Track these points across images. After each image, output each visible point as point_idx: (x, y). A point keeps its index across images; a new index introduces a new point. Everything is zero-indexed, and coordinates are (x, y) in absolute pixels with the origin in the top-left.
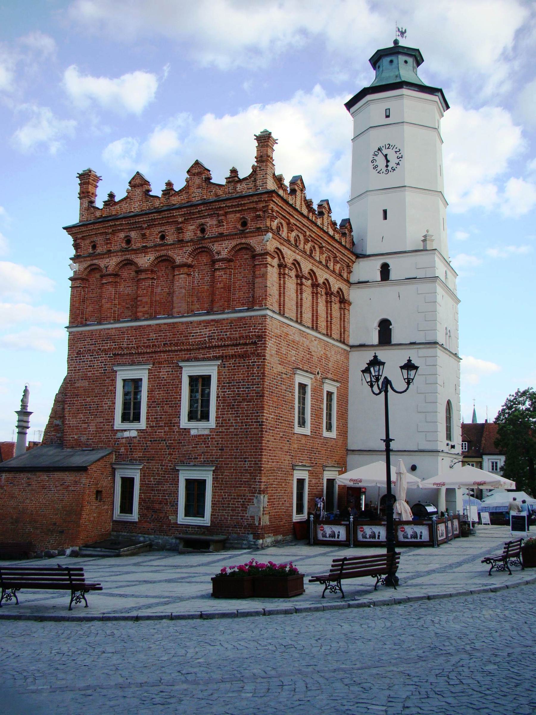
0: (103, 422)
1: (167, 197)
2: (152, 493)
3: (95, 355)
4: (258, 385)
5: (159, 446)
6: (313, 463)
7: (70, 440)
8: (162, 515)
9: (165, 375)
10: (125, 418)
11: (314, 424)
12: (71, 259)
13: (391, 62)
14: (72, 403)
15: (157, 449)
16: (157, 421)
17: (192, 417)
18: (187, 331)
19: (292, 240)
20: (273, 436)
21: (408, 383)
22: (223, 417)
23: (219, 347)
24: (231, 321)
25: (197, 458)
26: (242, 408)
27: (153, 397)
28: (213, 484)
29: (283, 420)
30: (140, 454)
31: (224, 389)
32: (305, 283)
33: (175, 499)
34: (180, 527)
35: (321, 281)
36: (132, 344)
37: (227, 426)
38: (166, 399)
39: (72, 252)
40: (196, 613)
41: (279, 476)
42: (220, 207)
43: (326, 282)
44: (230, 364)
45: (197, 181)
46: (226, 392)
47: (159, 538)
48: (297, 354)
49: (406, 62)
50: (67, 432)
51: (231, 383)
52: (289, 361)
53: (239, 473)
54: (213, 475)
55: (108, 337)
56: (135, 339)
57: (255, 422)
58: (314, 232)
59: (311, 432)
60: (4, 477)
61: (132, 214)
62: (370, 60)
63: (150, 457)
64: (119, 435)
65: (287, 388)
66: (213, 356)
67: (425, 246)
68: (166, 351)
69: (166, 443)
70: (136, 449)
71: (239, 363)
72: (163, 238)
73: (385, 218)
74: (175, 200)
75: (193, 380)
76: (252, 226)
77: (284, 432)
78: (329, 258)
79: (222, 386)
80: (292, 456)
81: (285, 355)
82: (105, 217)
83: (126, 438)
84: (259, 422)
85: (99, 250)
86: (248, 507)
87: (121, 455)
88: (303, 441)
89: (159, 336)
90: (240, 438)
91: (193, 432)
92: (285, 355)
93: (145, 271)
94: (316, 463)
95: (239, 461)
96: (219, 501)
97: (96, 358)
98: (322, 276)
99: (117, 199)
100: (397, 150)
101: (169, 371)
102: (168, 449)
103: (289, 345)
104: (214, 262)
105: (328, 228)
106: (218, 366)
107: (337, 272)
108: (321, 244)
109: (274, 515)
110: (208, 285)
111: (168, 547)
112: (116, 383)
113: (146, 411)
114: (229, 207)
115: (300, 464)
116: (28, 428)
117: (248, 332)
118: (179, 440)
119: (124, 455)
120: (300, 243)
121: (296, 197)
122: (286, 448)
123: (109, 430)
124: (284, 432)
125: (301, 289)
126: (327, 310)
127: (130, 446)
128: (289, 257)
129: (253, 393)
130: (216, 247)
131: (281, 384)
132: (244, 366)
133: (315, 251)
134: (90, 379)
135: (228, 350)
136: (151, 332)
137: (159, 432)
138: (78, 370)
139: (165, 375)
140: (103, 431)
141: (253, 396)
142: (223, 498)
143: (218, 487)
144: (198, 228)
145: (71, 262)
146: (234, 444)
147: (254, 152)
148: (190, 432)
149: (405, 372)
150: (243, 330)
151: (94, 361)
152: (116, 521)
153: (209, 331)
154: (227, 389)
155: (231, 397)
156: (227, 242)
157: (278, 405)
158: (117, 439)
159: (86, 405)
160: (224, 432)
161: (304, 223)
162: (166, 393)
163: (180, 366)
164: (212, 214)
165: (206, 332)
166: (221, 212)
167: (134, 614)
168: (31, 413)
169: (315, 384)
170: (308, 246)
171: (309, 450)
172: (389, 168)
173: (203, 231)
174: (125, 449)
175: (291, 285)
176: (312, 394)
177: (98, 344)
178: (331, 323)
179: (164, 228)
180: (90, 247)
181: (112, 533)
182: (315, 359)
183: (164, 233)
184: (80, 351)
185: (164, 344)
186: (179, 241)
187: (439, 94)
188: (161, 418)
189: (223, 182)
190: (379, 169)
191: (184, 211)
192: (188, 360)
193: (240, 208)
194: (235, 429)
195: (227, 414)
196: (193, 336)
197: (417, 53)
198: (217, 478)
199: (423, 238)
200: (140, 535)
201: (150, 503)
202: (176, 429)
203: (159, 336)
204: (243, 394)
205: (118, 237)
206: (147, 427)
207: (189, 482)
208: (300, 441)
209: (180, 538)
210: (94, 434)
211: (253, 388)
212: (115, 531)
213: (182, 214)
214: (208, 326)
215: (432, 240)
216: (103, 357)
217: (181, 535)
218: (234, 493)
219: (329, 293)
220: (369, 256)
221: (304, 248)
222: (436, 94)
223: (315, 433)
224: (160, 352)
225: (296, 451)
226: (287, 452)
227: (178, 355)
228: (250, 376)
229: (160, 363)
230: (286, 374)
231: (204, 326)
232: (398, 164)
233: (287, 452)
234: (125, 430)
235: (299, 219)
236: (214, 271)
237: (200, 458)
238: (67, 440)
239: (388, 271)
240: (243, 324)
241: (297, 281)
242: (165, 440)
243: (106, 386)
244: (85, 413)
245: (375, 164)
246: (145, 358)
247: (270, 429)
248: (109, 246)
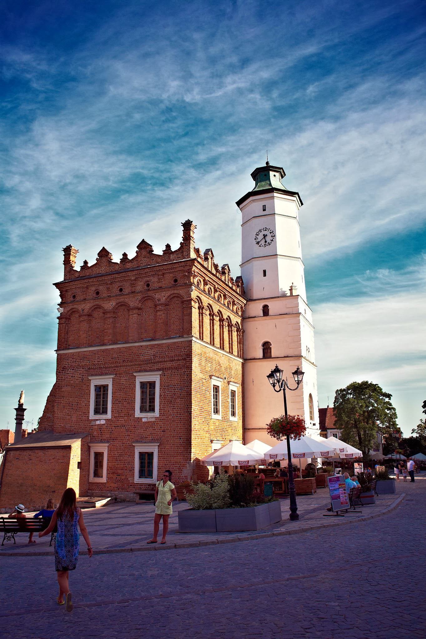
0: (82, 415)
1: (123, 263)
2: (116, 462)
3: (76, 369)
4: (187, 387)
5: (120, 430)
6: (223, 439)
7: (58, 428)
8: (123, 477)
9: (124, 381)
10: (97, 412)
11: (223, 412)
12: (58, 305)
14: (60, 402)
15: (119, 432)
16: (119, 413)
17: (142, 410)
18: (139, 352)
19: (207, 290)
20: (198, 421)
21: (298, 384)
22: (164, 409)
23: (161, 362)
24: (168, 345)
25: (147, 438)
26: (177, 403)
27: (116, 396)
28: (158, 455)
29: (204, 410)
30: (108, 436)
31: (165, 390)
32: (216, 319)
33: (132, 466)
34: (136, 486)
35: (225, 317)
36: (101, 362)
37: (167, 415)
38: (125, 398)
39: (59, 300)
40: (172, 545)
41: (203, 448)
42: (160, 270)
43: (228, 318)
44: (168, 373)
45: (144, 252)
46: (166, 392)
47: (122, 494)
48: (212, 366)
49: (275, 176)
50: (56, 422)
51: (169, 386)
52: (207, 371)
53: (176, 447)
54: (158, 449)
55: (84, 357)
56: (103, 358)
57: (186, 412)
58: (220, 285)
59: (222, 417)
60: (12, 454)
61: (100, 275)
62: (251, 175)
63: (115, 438)
64: (93, 423)
65: (206, 389)
66: (157, 369)
67: (291, 293)
68: (125, 366)
69: (125, 428)
70: (105, 432)
71: (174, 373)
72: (121, 290)
73: (265, 275)
74: (129, 265)
75: (143, 385)
76: (181, 281)
77: (205, 418)
78: (230, 302)
79: (163, 388)
80: (211, 434)
81: (205, 366)
82: (81, 277)
83: (97, 425)
84: (189, 412)
85: (78, 298)
86: (183, 470)
87: (94, 437)
88: (217, 424)
89: (120, 355)
90: (176, 423)
91: (143, 420)
92: (205, 366)
93: (109, 312)
94: (226, 439)
95: (176, 439)
96: (163, 466)
97: (76, 371)
98: (226, 313)
99: (90, 265)
100: (271, 231)
101: (127, 379)
102: (127, 432)
103: (207, 360)
104: (156, 306)
105: (228, 282)
106: (160, 375)
107: (235, 311)
109: (200, 475)
110: (152, 321)
111: (128, 500)
112: (90, 387)
113: (111, 406)
114: (165, 270)
115: (216, 439)
116: (23, 419)
117: (180, 352)
118: (135, 425)
119: (96, 437)
120: (211, 293)
121: (208, 263)
122: (206, 429)
123: (85, 420)
124: (205, 418)
125: (213, 323)
127: (100, 431)
128: (205, 302)
129: (184, 393)
130: (157, 296)
131: (202, 386)
132: (178, 374)
133: (221, 297)
134: (72, 386)
135: (167, 364)
136: (114, 353)
137: (120, 421)
138: (64, 379)
139: (124, 381)
140: (81, 420)
141: (185, 394)
142: (165, 465)
143: (162, 457)
144: (145, 283)
145: (59, 307)
146: (172, 427)
147: (181, 234)
148: (142, 420)
149: (296, 376)
150: (177, 351)
151: (75, 373)
152: (91, 483)
153: (154, 351)
154: (167, 390)
155: (170, 395)
156: (164, 292)
157: (200, 400)
158: (91, 426)
159: (70, 403)
160: (165, 419)
161: (214, 279)
162: (125, 394)
163: (134, 376)
164: (153, 275)
165: (152, 352)
166: (160, 273)
167: (129, 547)
168: (25, 409)
169: (223, 386)
170: (217, 295)
171: (221, 430)
172: (267, 243)
173: (148, 285)
174: (97, 433)
175: (207, 319)
176: (222, 392)
177: (78, 361)
179: (121, 284)
180: (72, 297)
181: (88, 491)
182: (223, 369)
183: (122, 287)
184: (65, 366)
185: (123, 361)
186: (132, 292)
187: (297, 196)
188: (121, 411)
189: (161, 253)
190: (260, 244)
191: (136, 272)
192: (140, 371)
193: (173, 271)
194: (172, 417)
195: (167, 407)
196: (143, 355)
197: (281, 170)
198: (161, 451)
199: (290, 288)
200: (108, 492)
201: (115, 469)
202: (132, 418)
203: (120, 355)
204: (178, 393)
205: (91, 290)
206: (112, 417)
207: (141, 454)
208: (215, 424)
209: (137, 493)
210: (75, 423)
211: (184, 389)
212: (90, 490)
213: (134, 275)
214: (152, 348)
216: (81, 370)
217: (137, 491)
218: (173, 460)
219: (230, 325)
221: (214, 296)
222: (295, 196)
223: (225, 418)
224: (121, 366)
225: (213, 431)
226: (207, 432)
227: (133, 368)
228: (182, 381)
229: (120, 374)
230: (206, 380)
231: (150, 348)
232: (272, 240)
233: (207, 432)
234: (97, 420)
235: (211, 277)
236: (156, 312)
237: (149, 438)
238: (56, 428)
240: (177, 347)
241: (210, 318)
242: (124, 426)
243: (83, 390)
244: (69, 408)
246: (110, 370)
247: (196, 417)
248: (84, 296)
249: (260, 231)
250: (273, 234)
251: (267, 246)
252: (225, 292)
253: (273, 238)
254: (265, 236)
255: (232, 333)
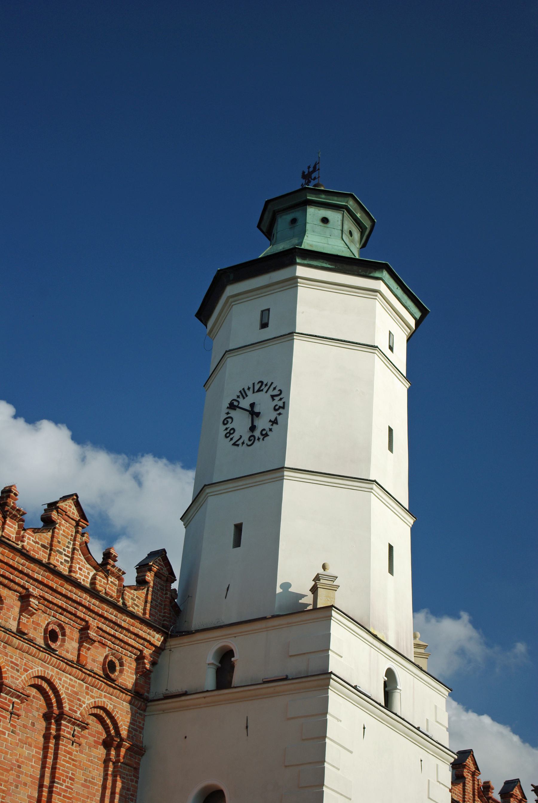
13: (294, 221)
49: (325, 220)
73: (237, 543)
100: (276, 392)
108: (23, 587)
126: (45, 757)
172: (257, 433)
178: (50, 792)
187: (385, 275)
190: (236, 436)
197: (351, 204)
215: (335, 588)
220: (198, 631)
222: (377, 275)
232: (275, 422)
239: (232, 667)
245: (230, 426)
249: (243, 394)
250: (281, 399)
251: (256, 441)
252: (27, 585)
253: (280, 414)
254: (253, 413)
255: (57, 745)
